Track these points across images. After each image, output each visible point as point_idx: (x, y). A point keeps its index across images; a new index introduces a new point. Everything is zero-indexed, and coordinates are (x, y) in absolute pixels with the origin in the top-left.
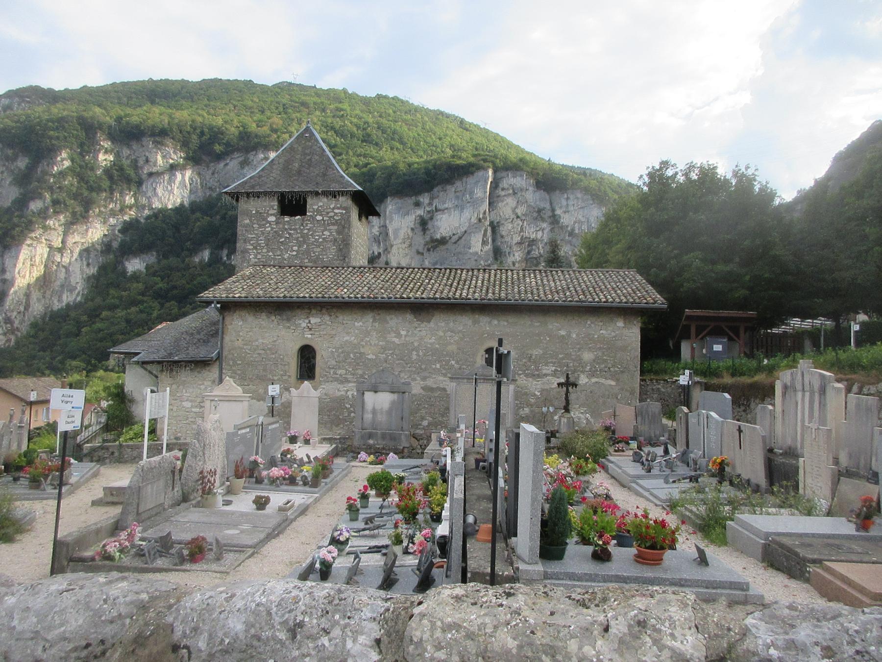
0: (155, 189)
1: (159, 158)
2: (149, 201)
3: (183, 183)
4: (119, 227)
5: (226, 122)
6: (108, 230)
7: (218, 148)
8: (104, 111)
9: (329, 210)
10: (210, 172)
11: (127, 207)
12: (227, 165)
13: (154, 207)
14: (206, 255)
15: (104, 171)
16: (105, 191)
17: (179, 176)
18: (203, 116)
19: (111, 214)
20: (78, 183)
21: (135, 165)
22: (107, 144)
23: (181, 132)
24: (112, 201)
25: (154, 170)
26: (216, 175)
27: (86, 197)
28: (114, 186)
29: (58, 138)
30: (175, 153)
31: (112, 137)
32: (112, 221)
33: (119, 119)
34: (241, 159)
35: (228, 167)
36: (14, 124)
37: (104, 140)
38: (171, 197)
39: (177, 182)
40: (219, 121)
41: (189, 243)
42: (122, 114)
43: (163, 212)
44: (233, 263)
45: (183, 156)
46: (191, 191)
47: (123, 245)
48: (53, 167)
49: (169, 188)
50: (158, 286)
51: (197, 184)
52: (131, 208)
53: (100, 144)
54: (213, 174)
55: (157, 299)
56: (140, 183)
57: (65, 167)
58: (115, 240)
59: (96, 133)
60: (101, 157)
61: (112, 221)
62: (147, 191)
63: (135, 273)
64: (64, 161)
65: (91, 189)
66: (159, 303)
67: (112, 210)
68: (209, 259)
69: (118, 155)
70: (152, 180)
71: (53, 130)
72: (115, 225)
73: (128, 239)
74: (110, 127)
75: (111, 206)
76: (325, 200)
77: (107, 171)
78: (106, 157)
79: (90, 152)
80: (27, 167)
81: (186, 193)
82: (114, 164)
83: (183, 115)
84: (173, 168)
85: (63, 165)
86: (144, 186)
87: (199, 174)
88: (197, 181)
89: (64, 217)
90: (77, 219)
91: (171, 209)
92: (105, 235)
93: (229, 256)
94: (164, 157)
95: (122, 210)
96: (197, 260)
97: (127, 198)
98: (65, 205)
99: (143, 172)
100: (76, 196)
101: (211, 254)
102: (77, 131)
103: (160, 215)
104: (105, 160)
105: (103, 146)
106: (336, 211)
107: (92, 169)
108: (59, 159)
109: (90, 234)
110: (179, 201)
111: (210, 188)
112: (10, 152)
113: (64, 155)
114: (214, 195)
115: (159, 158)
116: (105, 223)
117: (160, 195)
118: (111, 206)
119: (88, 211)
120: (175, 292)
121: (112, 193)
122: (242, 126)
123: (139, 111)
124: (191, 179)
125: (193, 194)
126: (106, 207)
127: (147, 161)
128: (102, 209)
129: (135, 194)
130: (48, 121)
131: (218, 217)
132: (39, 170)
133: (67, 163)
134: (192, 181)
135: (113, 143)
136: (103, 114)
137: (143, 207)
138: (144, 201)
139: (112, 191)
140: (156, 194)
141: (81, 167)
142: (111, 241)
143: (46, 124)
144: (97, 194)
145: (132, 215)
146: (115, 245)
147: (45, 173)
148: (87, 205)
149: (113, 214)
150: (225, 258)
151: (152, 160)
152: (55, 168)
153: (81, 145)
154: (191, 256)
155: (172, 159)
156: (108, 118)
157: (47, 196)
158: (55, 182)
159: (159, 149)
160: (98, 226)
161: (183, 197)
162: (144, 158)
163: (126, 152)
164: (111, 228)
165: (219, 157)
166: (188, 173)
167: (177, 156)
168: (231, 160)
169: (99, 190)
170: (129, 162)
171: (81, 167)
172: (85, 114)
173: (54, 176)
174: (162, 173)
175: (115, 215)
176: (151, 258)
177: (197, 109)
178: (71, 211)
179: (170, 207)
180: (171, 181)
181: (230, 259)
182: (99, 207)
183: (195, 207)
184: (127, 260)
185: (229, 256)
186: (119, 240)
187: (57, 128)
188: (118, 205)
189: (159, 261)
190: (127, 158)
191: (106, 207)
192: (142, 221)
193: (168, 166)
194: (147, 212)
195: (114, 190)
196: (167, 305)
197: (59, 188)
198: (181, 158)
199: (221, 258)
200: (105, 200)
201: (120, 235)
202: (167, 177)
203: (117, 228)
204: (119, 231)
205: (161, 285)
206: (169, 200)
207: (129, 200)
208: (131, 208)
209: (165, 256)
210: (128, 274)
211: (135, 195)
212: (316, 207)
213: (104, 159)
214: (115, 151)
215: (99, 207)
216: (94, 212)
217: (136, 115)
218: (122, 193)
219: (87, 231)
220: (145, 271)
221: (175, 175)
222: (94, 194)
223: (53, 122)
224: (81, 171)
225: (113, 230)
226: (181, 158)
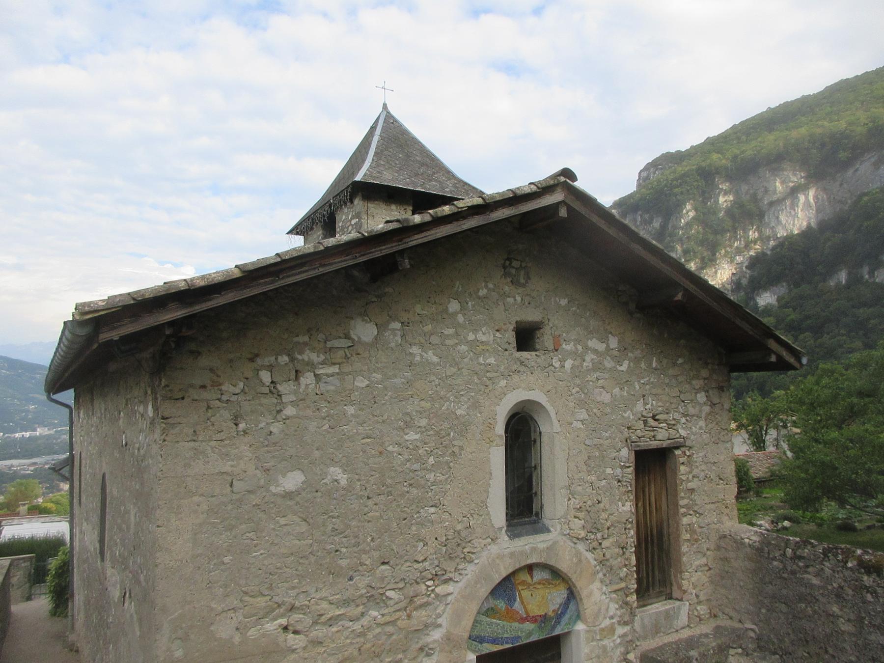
0: (778, 218)
1: (778, 184)
2: (773, 231)
3: (807, 204)
4: (746, 264)
5: (850, 124)
6: (736, 269)
7: (842, 155)
8: (720, 156)
9: (348, 224)
10: (838, 183)
11: (752, 241)
12: (857, 170)
13: (779, 236)
14: (843, 276)
15: (725, 212)
16: (729, 231)
17: (802, 198)
18: (822, 126)
19: (737, 253)
20: (704, 229)
21: (755, 199)
22: (725, 186)
23: (798, 151)
24: (736, 239)
25: (775, 198)
26: (845, 185)
27: (712, 241)
28: (737, 225)
29: (682, 193)
30: (795, 175)
31: (729, 178)
32: (739, 259)
33: (735, 157)
34: (873, 160)
35: (859, 172)
36: (648, 192)
37: (722, 183)
38: (796, 222)
39: (801, 206)
40: (842, 125)
41: (820, 267)
42: (738, 152)
43: (790, 238)
44: (877, 280)
45: (803, 175)
46: (817, 210)
47: (752, 280)
48: (681, 221)
49: (793, 213)
50: (789, 318)
51: (823, 200)
52: (755, 242)
53: (719, 188)
54: (841, 185)
55: (790, 332)
56: (761, 215)
57: (690, 217)
58: (744, 277)
59: (715, 178)
60: (721, 199)
61: (739, 259)
62: (770, 222)
63: (766, 307)
64: (689, 212)
65: (716, 233)
66: (792, 335)
67: (737, 248)
68: (846, 281)
69: (737, 194)
70: (773, 209)
71: (678, 187)
72: (742, 263)
73: (755, 274)
74: (726, 168)
75: (736, 245)
76: (346, 210)
77: (729, 212)
78: (726, 198)
79: (711, 198)
80: (661, 226)
81: (812, 213)
82: (734, 203)
83: (800, 132)
84: (794, 192)
85: (689, 216)
86: (766, 217)
87: (825, 190)
88: (823, 197)
89: (695, 264)
90: (706, 263)
91: (797, 234)
92: (733, 274)
93: (871, 273)
94: (782, 183)
95: (747, 246)
96: (832, 283)
97: (751, 233)
98: (694, 252)
99: (763, 203)
100: (702, 243)
101: (849, 274)
102: (697, 181)
103: (788, 243)
104: (726, 201)
105: (722, 189)
106: (353, 222)
107: (715, 213)
108: (684, 211)
109: (719, 275)
110: (805, 224)
111: (840, 202)
112: (647, 216)
113: (688, 206)
114: (846, 208)
115: (778, 184)
116: (732, 262)
117: (784, 222)
118: (736, 245)
119: (715, 255)
120: (809, 322)
121: (736, 232)
122: (870, 122)
123: (754, 143)
124: (816, 197)
125: (820, 212)
126: (731, 246)
127: (766, 191)
128: (728, 249)
129: (758, 227)
130: (673, 180)
131: (852, 232)
132: (670, 226)
133: (692, 214)
134: (818, 199)
135: (731, 183)
136: (719, 158)
137: (768, 238)
138: (768, 232)
139: (734, 230)
140: (779, 222)
141: (704, 214)
142: (740, 279)
143: (671, 184)
144: (722, 236)
145: (758, 249)
146: (744, 282)
147: (675, 227)
148: (713, 248)
149: (739, 251)
150: (867, 276)
151: (771, 189)
152: (683, 221)
153: (704, 192)
154: (824, 280)
155: (792, 182)
156: (724, 161)
157: (679, 247)
158: (683, 234)
159: (776, 175)
160: (726, 266)
161: (810, 218)
162: (762, 190)
163: (744, 188)
164: (739, 266)
165: (846, 165)
166: (811, 193)
167: (795, 177)
168: (861, 165)
169: (724, 231)
170: (748, 197)
171: (704, 214)
172: (703, 164)
173: (682, 228)
174: (784, 199)
175: (740, 252)
176: (782, 289)
177: (817, 121)
178: (699, 256)
179: (796, 232)
180: (793, 206)
181: (874, 277)
182: (725, 248)
183: (824, 227)
184: (757, 295)
185: (871, 273)
186: (748, 276)
187: (681, 185)
188: (742, 242)
189: (790, 290)
190: (747, 193)
191: (731, 246)
192: (769, 253)
193: (788, 190)
194: (772, 243)
195: (737, 228)
196: (801, 337)
197: (688, 237)
198: (802, 177)
199: (862, 277)
200: (730, 240)
201: (748, 271)
202: (788, 202)
203: (745, 265)
204: (746, 267)
205: (793, 316)
206: (794, 225)
207: (753, 234)
208: (755, 242)
209: (797, 285)
210: (760, 309)
211: (759, 230)
212: (340, 225)
213: (724, 201)
214: (734, 190)
215: (725, 248)
216: (720, 253)
217: (749, 150)
218: (745, 231)
219: (716, 272)
220: (777, 303)
221: (797, 198)
222: (719, 237)
223: (677, 181)
224: (704, 217)
225: (741, 268)
226: (802, 177)
